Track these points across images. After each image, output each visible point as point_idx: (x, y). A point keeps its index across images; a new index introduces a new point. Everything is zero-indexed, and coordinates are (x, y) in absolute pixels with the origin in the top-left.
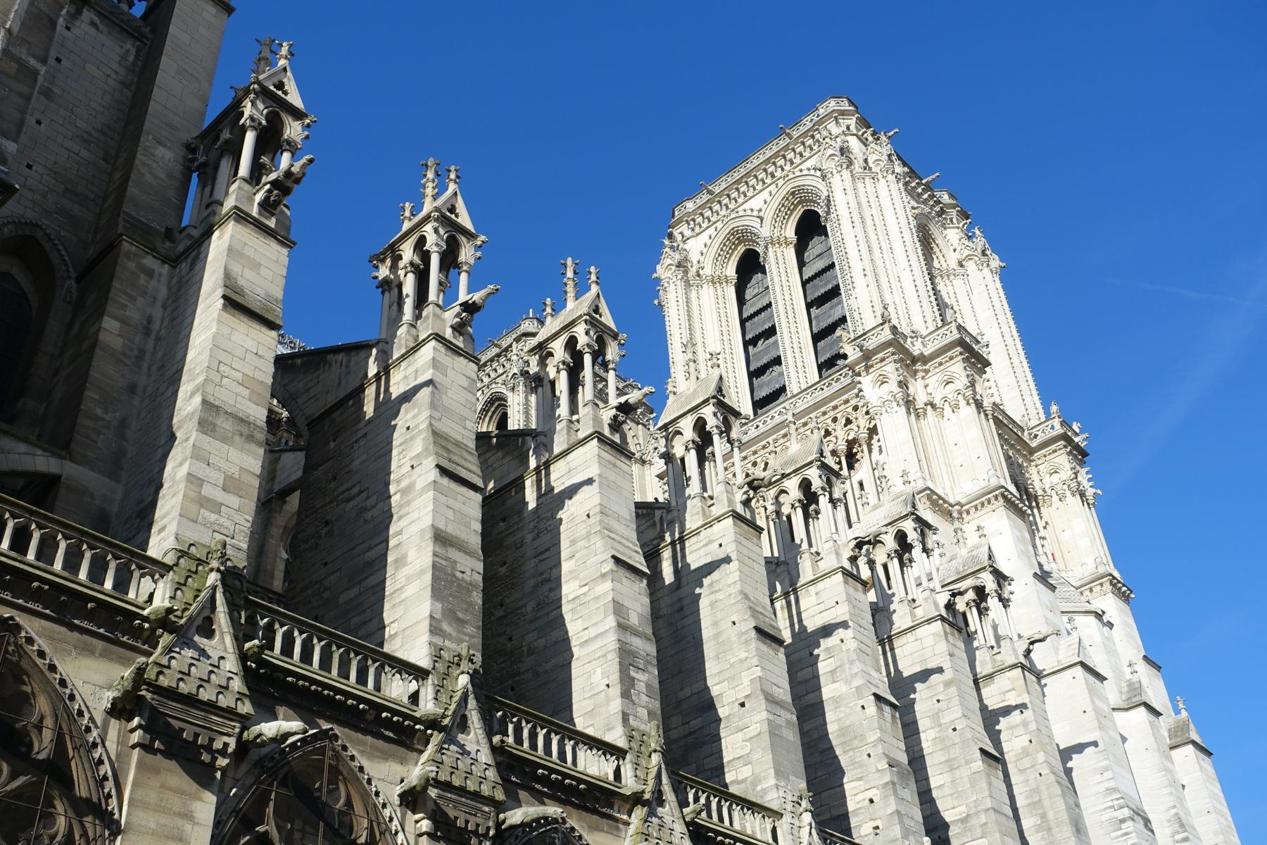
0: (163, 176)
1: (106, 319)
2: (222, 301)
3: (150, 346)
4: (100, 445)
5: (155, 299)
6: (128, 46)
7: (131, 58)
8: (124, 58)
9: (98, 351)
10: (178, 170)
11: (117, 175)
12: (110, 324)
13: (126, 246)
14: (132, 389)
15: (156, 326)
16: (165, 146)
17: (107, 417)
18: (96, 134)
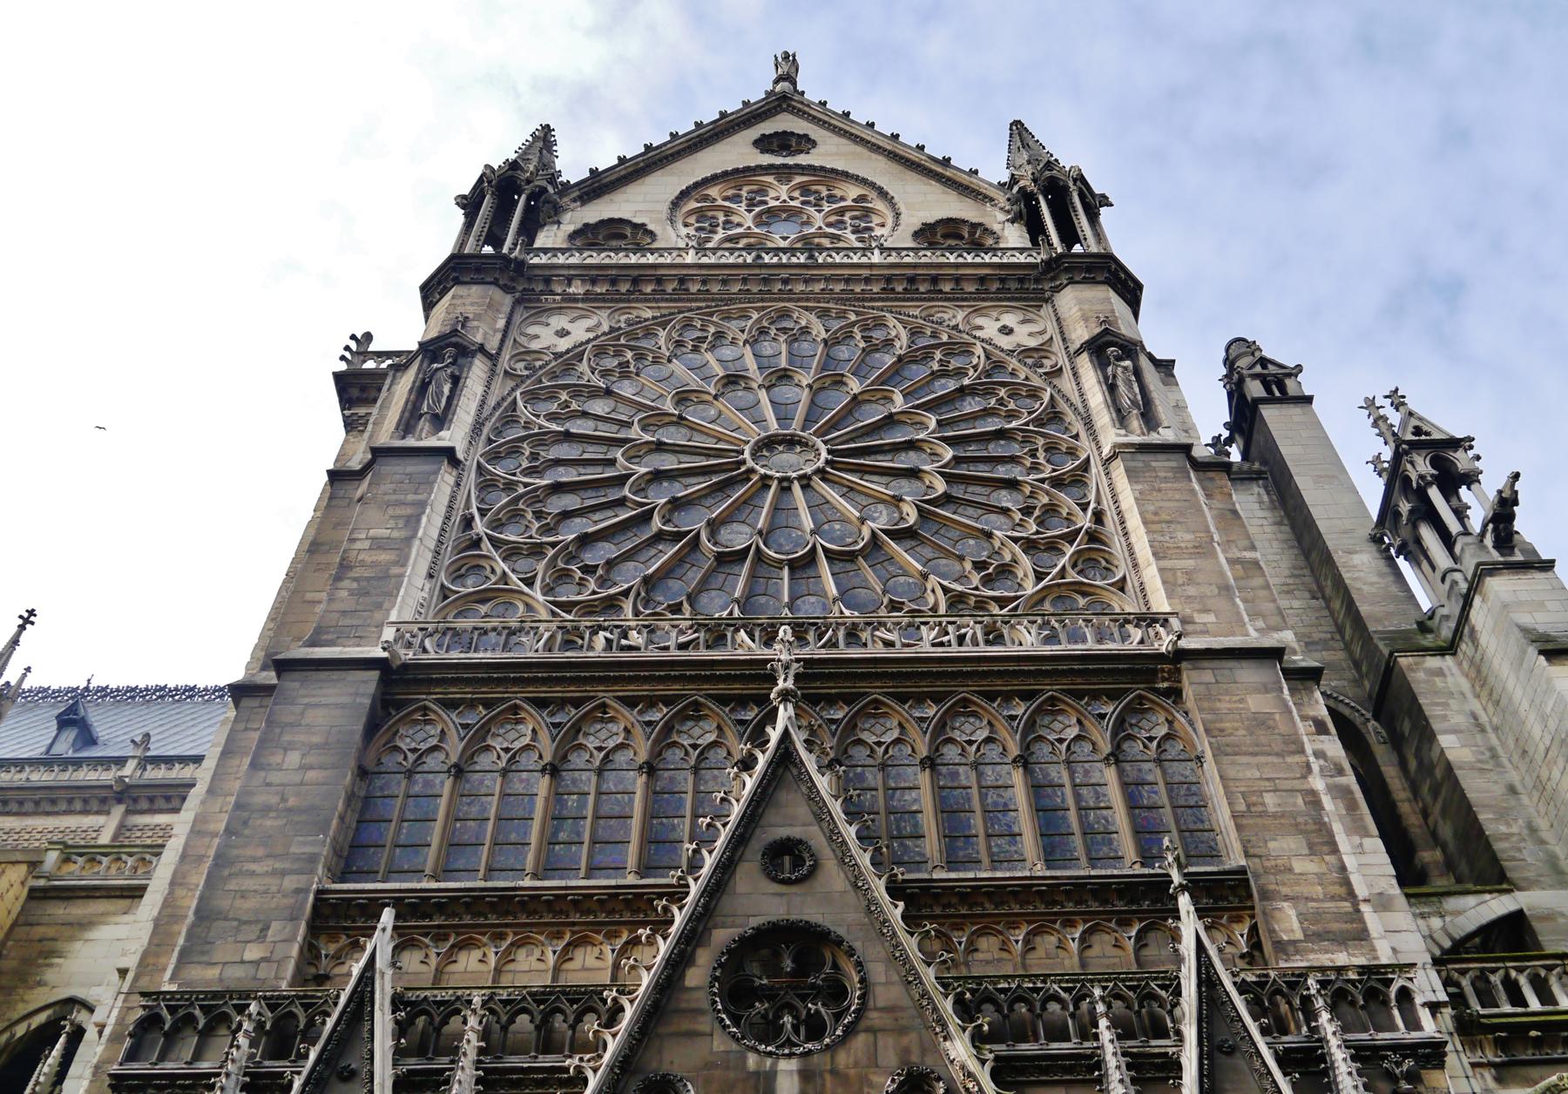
0: (1375, 579)
1: (1440, 737)
2: (1542, 658)
3: (1494, 741)
4: (1529, 860)
5: (1462, 694)
6: (1256, 490)
7: (1266, 498)
8: (1261, 502)
9: (1458, 772)
10: (1381, 565)
11: (1336, 604)
12: (1446, 741)
13: (1404, 661)
14: (1512, 790)
15: (1483, 718)
16: (1356, 552)
17: (1515, 830)
18: (1290, 581)
